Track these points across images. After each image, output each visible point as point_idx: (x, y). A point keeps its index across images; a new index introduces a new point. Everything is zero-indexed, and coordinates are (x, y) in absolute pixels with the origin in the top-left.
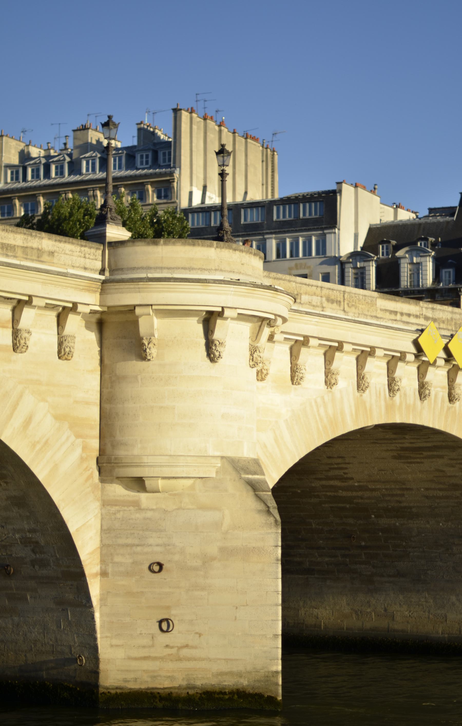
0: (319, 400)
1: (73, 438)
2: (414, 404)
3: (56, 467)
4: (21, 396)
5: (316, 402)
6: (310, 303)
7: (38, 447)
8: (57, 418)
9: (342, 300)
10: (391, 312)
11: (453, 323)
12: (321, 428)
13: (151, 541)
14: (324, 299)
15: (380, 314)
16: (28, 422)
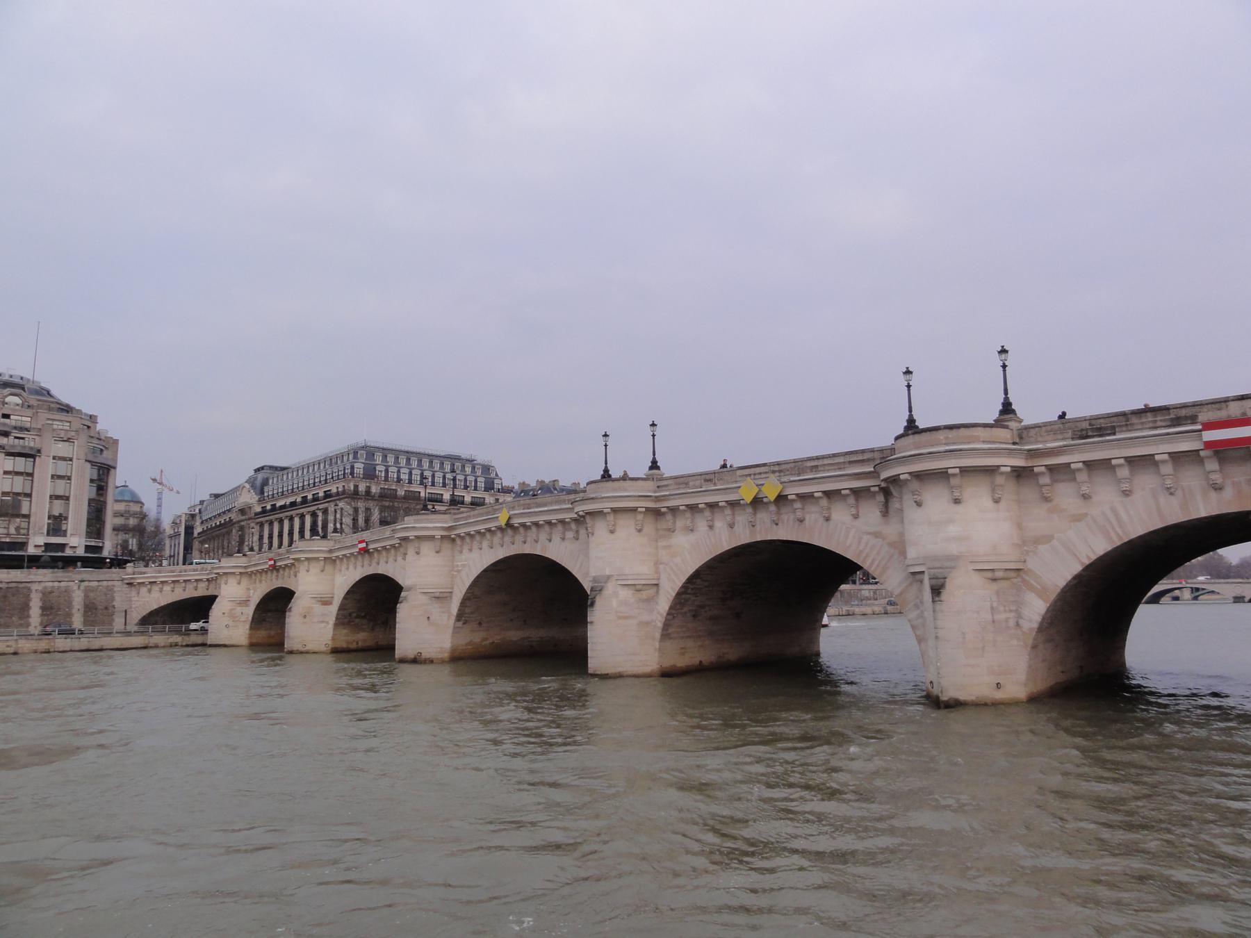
11: (796, 469)
14: (703, 481)
15: (739, 479)
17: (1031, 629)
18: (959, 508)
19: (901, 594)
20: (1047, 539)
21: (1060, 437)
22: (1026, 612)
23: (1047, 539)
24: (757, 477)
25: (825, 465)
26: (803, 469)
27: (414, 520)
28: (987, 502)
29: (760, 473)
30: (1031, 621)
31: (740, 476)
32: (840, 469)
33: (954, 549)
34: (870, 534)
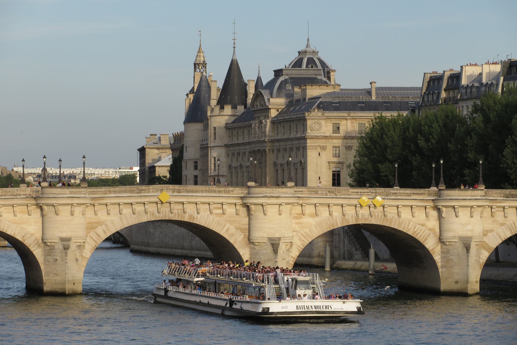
0: (327, 219)
1: (241, 233)
2: (368, 218)
3: (236, 240)
4: (226, 224)
5: (326, 220)
6: (322, 193)
7: (231, 235)
8: (236, 229)
9: (335, 191)
10: (356, 192)
11: (385, 193)
12: (328, 227)
13: (257, 257)
15: (350, 194)
16: (228, 230)
17: (483, 262)
18: (472, 219)
19: (432, 250)
20: (492, 231)
21: (499, 195)
22: (482, 257)
23: (492, 231)
24: (362, 194)
25: (401, 193)
26: (388, 193)
27: (70, 192)
28: (479, 217)
29: (364, 193)
30: (483, 260)
31: (351, 192)
32: (409, 196)
33: (469, 234)
34: (419, 224)
